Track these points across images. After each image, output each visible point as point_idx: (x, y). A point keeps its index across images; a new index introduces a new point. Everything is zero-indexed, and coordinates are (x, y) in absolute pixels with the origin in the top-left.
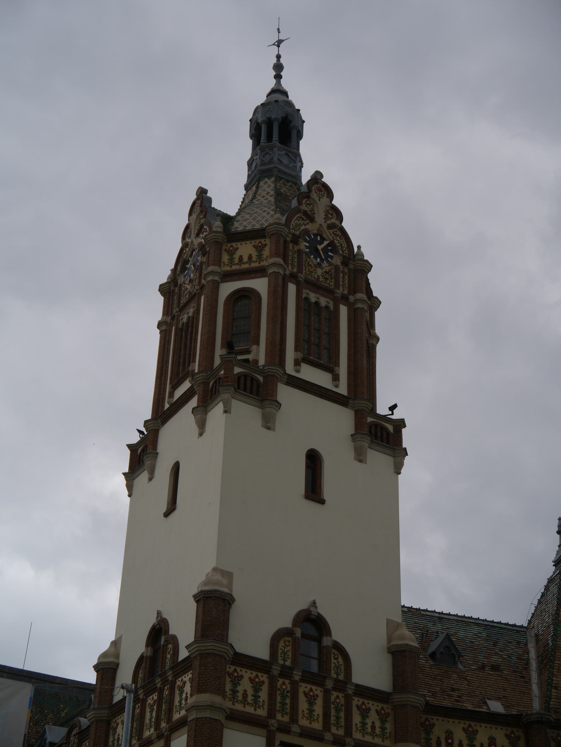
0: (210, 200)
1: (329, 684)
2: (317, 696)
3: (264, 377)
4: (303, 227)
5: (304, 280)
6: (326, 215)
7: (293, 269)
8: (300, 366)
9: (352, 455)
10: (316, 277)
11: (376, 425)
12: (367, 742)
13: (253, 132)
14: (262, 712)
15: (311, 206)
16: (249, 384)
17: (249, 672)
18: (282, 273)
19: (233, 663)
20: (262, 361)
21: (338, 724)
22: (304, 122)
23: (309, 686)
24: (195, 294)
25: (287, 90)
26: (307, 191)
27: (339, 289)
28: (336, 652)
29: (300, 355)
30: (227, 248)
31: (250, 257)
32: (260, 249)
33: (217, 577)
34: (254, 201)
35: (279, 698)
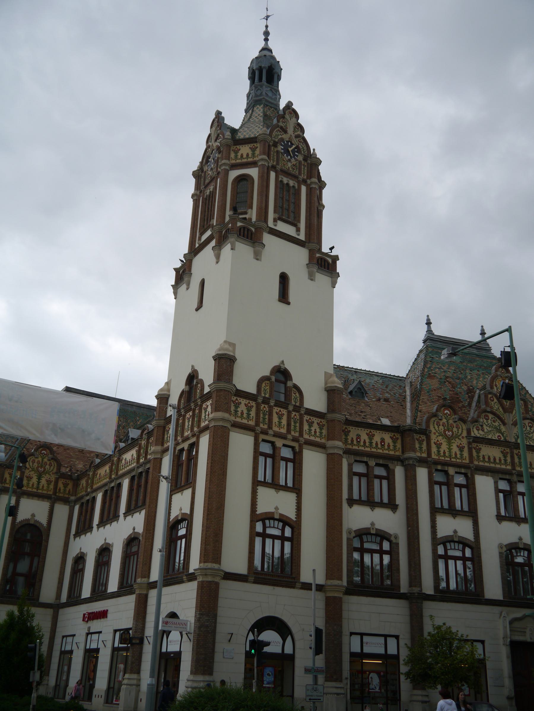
0: (223, 119)
1: (291, 408)
2: (284, 414)
3: (255, 229)
4: (280, 137)
5: (280, 170)
6: (294, 129)
7: (273, 162)
8: (277, 222)
9: (306, 276)
10: (287, 168)
11: (321, 259)
12: (312, 440)
13: (250, 75)
14: (252, 423)
15: (285, 123)
16: (246, 232)
17: (245, 400)
18: (267, 165)
19: (235, 395)
20: (254, 219)
21: (295, 430)
22: (282, 69)
23: (279, 409)
24: (214, 177)
25: (272, 48)
26: (283, 114)
27: (301, 175)
28: (295, 390)
29: (277, 216)
30: (234, 149)
31: (248, 155)
32: (253, 150)
33: (227, 346)
34: (250, 119)
35: (262, 415)
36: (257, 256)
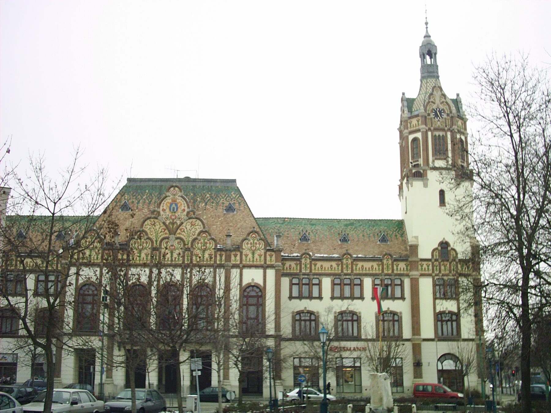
14: (430, 272)
29: (434, 158)
32: (418, 121)
36: (426, 185)
